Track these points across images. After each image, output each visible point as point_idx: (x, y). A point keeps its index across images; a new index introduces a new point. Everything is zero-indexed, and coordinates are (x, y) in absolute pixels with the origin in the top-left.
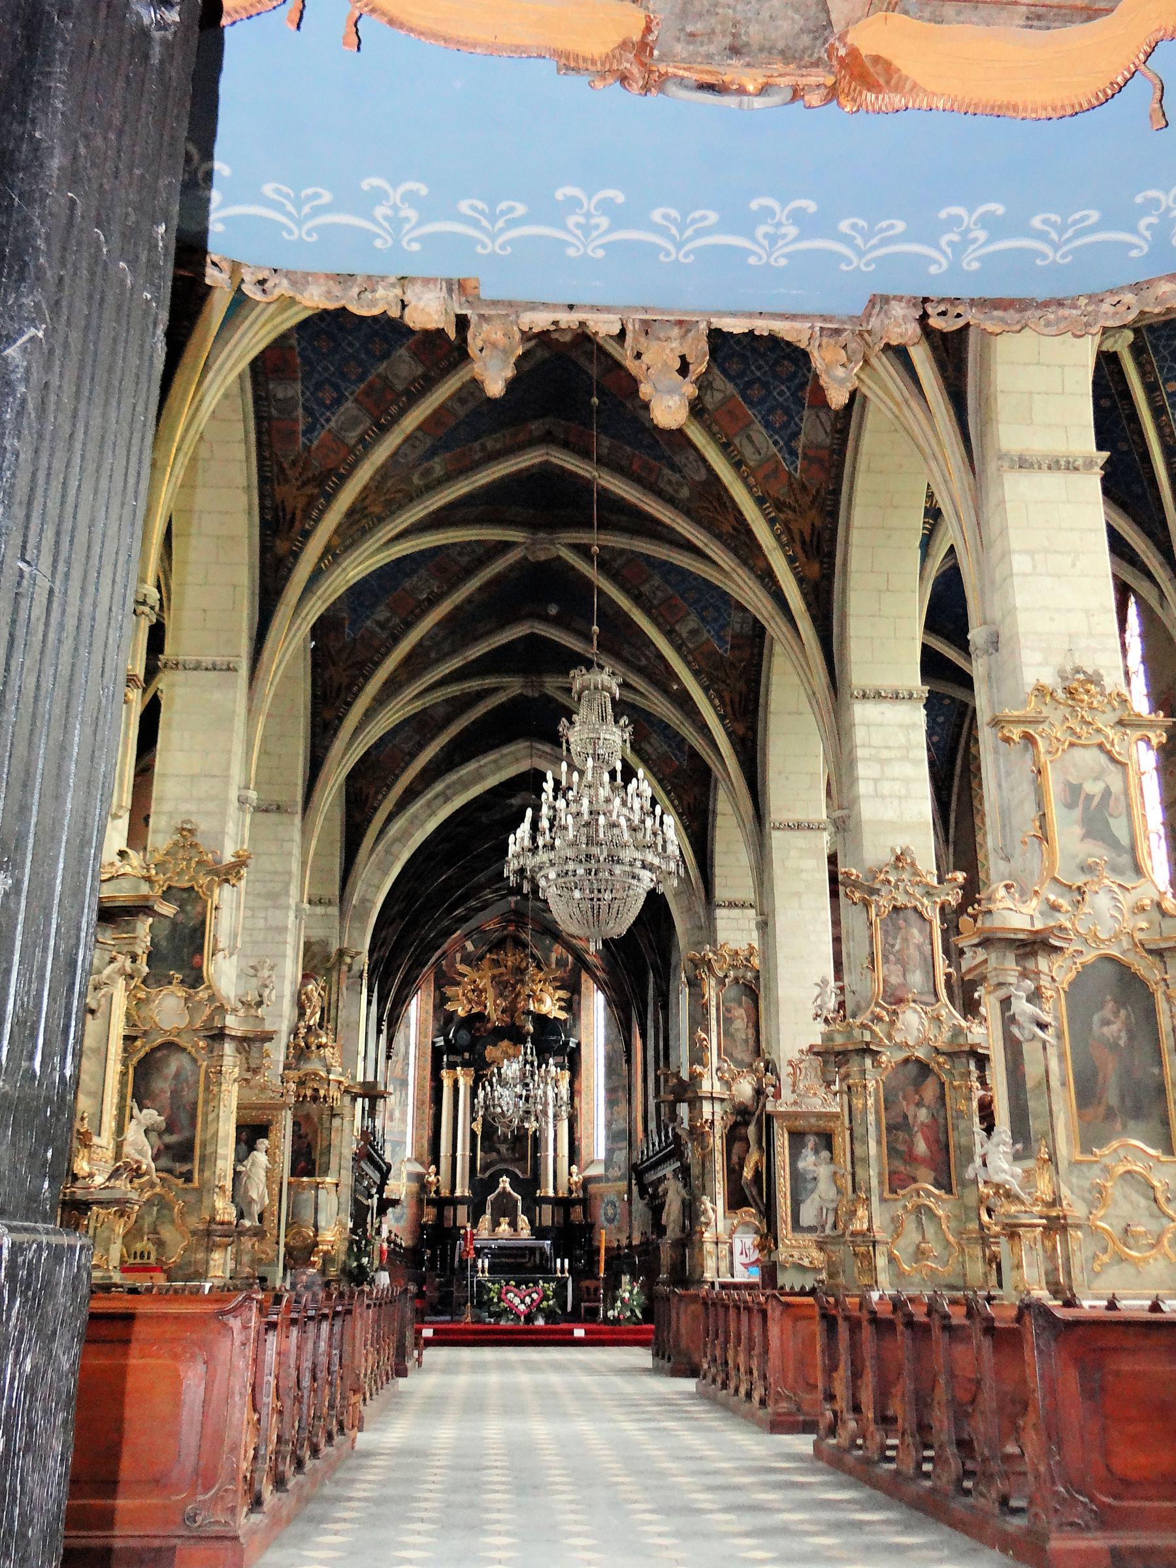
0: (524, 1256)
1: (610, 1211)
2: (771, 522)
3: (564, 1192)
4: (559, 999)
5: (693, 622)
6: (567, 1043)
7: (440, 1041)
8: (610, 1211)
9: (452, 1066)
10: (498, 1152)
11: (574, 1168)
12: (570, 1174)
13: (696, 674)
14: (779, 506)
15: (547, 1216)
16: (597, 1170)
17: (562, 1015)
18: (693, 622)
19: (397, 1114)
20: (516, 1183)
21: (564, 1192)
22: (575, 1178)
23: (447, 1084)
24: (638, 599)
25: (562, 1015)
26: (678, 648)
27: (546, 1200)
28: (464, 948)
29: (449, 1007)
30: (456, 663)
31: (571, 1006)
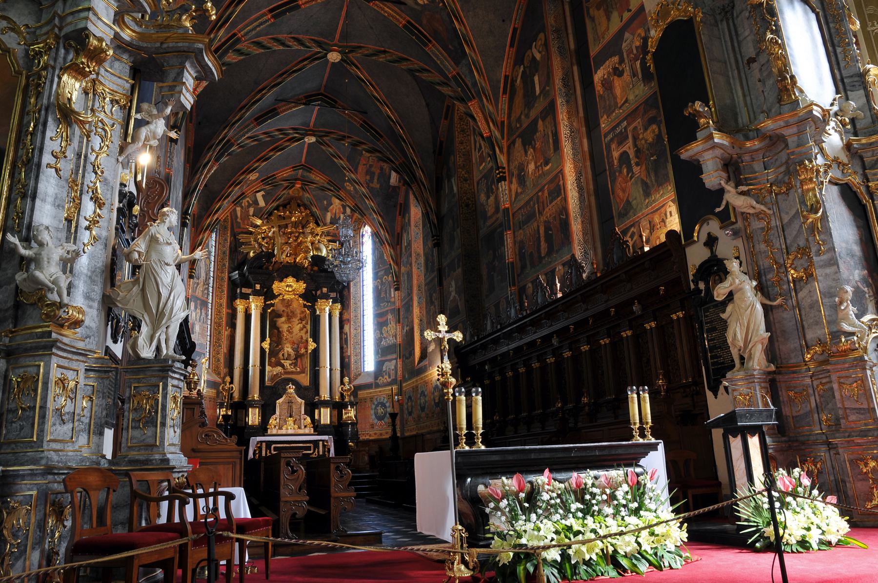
3: (337, 398)
7: (236, 275)
9: (246, 297)
10: (283, 366)
15: (325, 416)
20: (301, 391)
28: (256, 202)
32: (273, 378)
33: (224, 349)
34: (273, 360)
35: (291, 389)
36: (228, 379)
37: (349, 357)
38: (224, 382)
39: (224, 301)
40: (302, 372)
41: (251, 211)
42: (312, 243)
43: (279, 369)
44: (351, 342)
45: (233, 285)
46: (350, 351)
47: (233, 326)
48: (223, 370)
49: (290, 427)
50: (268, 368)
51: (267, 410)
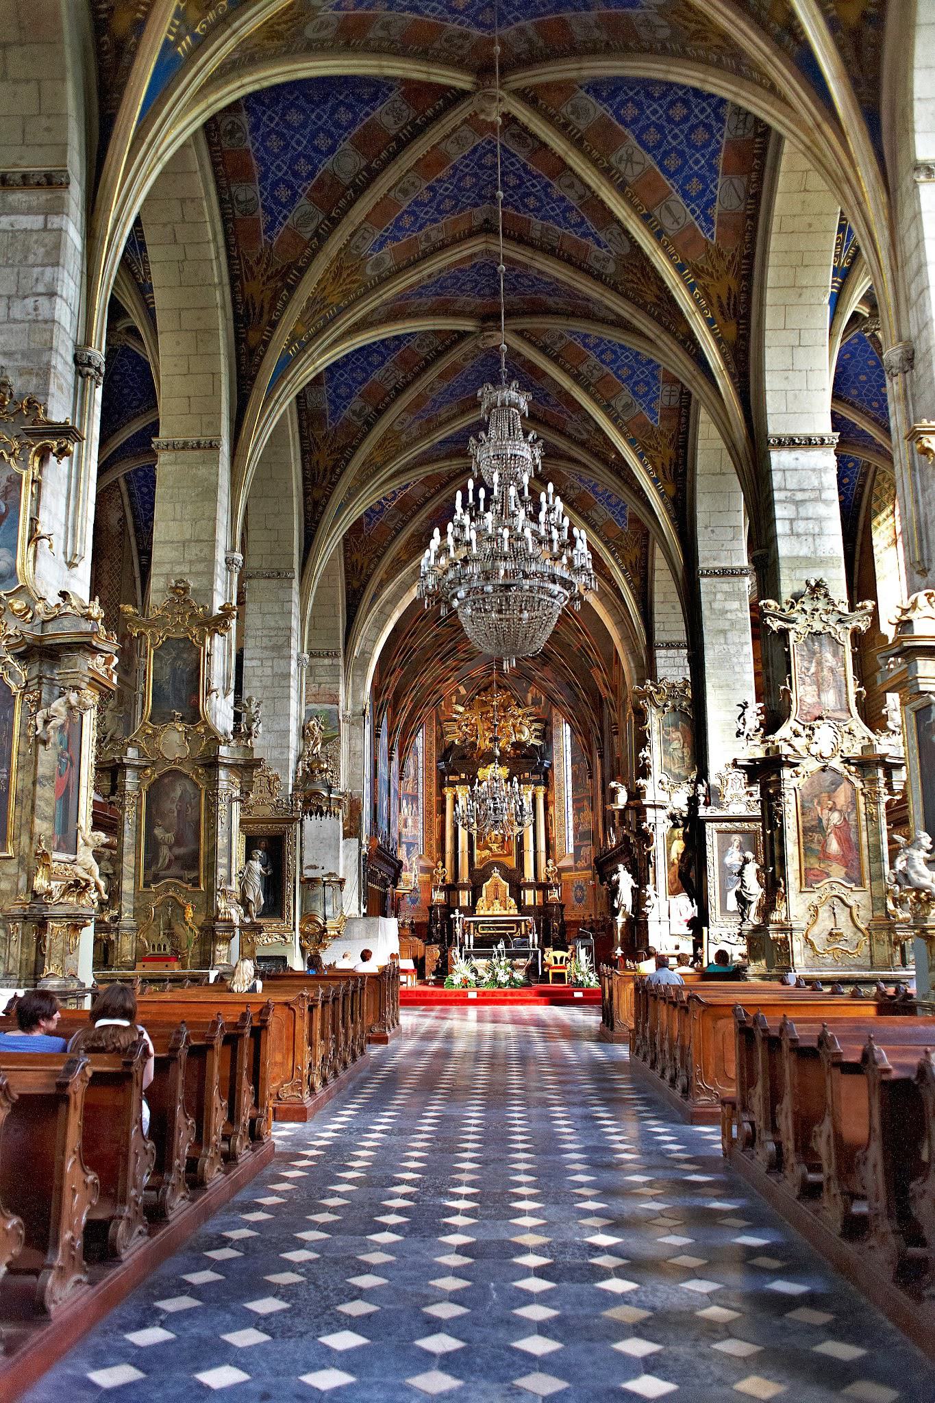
0: (512, 928)
1: (579, 893)
2: (691, 288)
3: (542, 878)
4: (535, 730)
5: (626, 396)
6: (541, 764)
8: (579, 893)
9: (452, 784)
10: (490, 849)
11: (550, 862)
13: (631, 443)
14: (698, 272)
16: (567, 862)
17: (538, 743)
18: (626, 396)
19: (410, 822)
20: (508, 875)
22: (551, 869)
23: (449, 796)
24: (576, 378)
25: (538, 743)
26: (614, 420)
27: (529, 886)
28: (458, 691)
29: (449, 738)
30: (424, 446)
31: (546, 735)
32: (481, 862)
33: (436, 835)
35: (496, 874)
36: (440, 864)
39: (434, 790)
40: (510, 854)
41: (454, 699)
42: (514, 726)
44: (556, 824)
45: (442, 774)
46: (555, 832)
47: (443, 811)
48: (436, 855)
49: (497, 909)
50: (476, 852)
51: (476, 894)
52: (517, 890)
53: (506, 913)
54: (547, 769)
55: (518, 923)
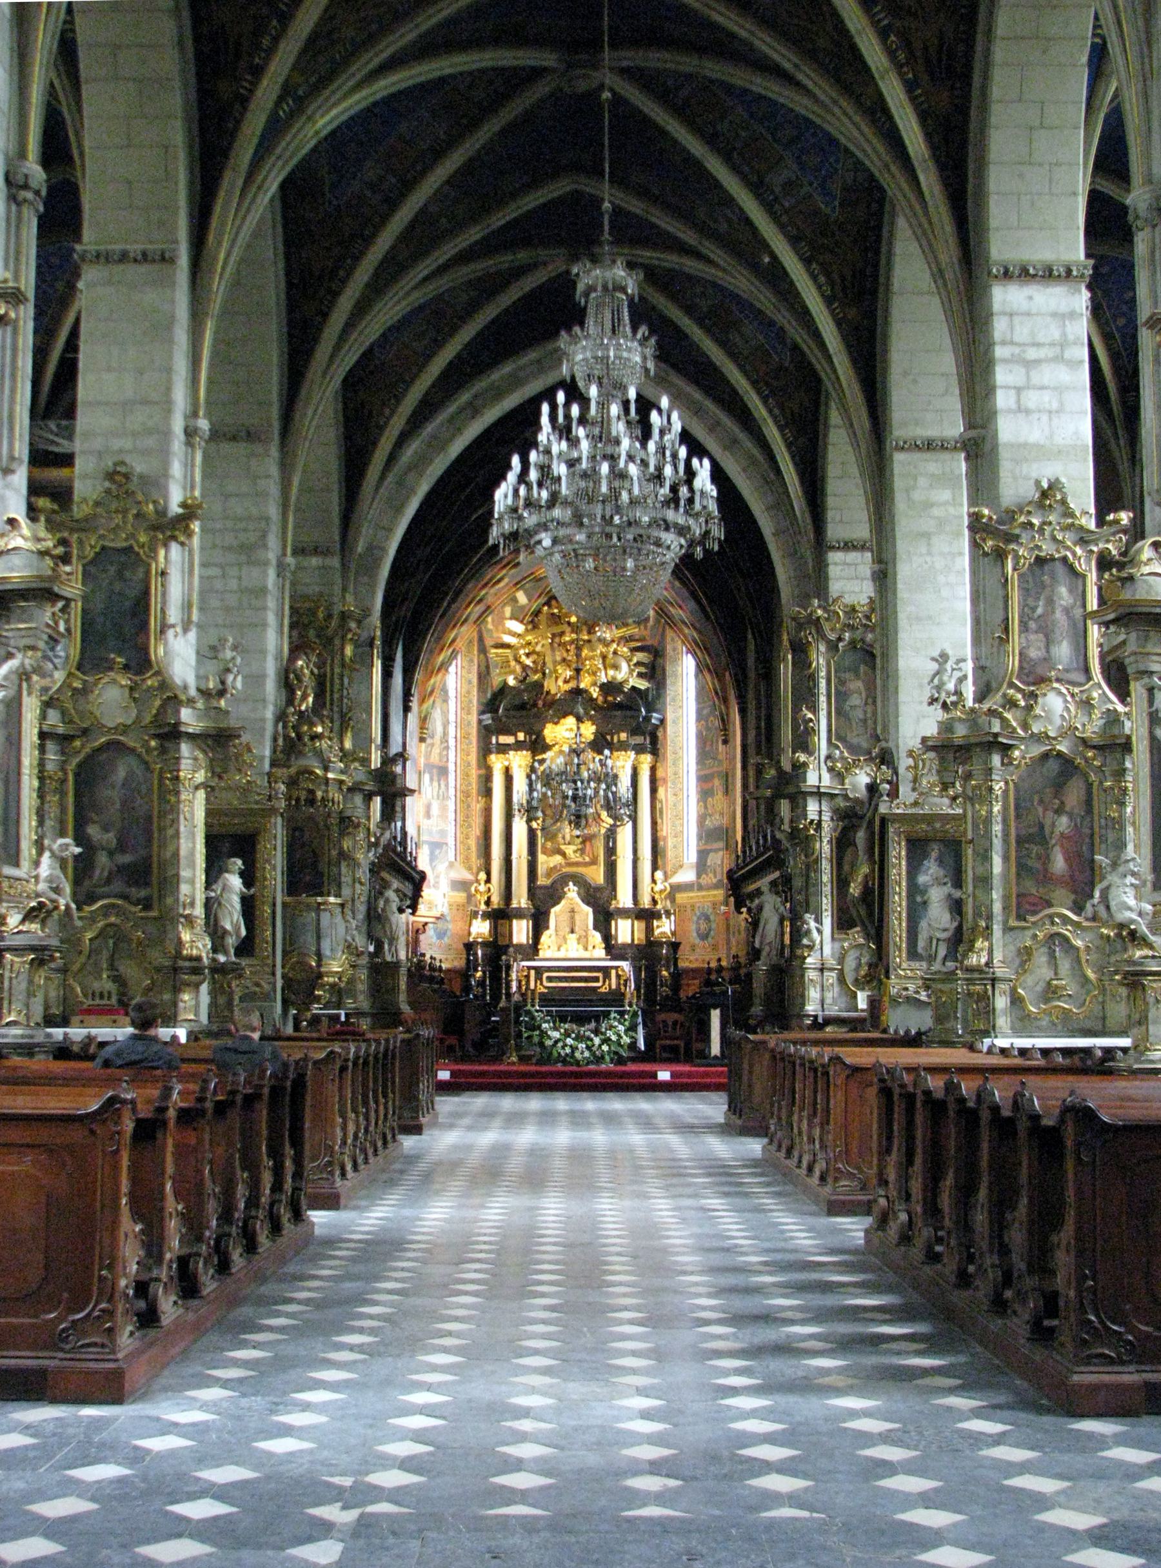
0: (596, 979)
3: (646, 902)
10: (563, 854)
11: (659, 875)
12: (654, 881)
21: (646, 902)
27: (624, 913)
34: (549, 845)
36: (482, 876)
37: (665, 839)
38: (478, 881)
40: (594, 862)
43: (558, 859)
48: (476, 862)
50: (541, 858)
52: (604, 918)
53: (587, 955)
54: (656, 727)
55: (606, 971)
